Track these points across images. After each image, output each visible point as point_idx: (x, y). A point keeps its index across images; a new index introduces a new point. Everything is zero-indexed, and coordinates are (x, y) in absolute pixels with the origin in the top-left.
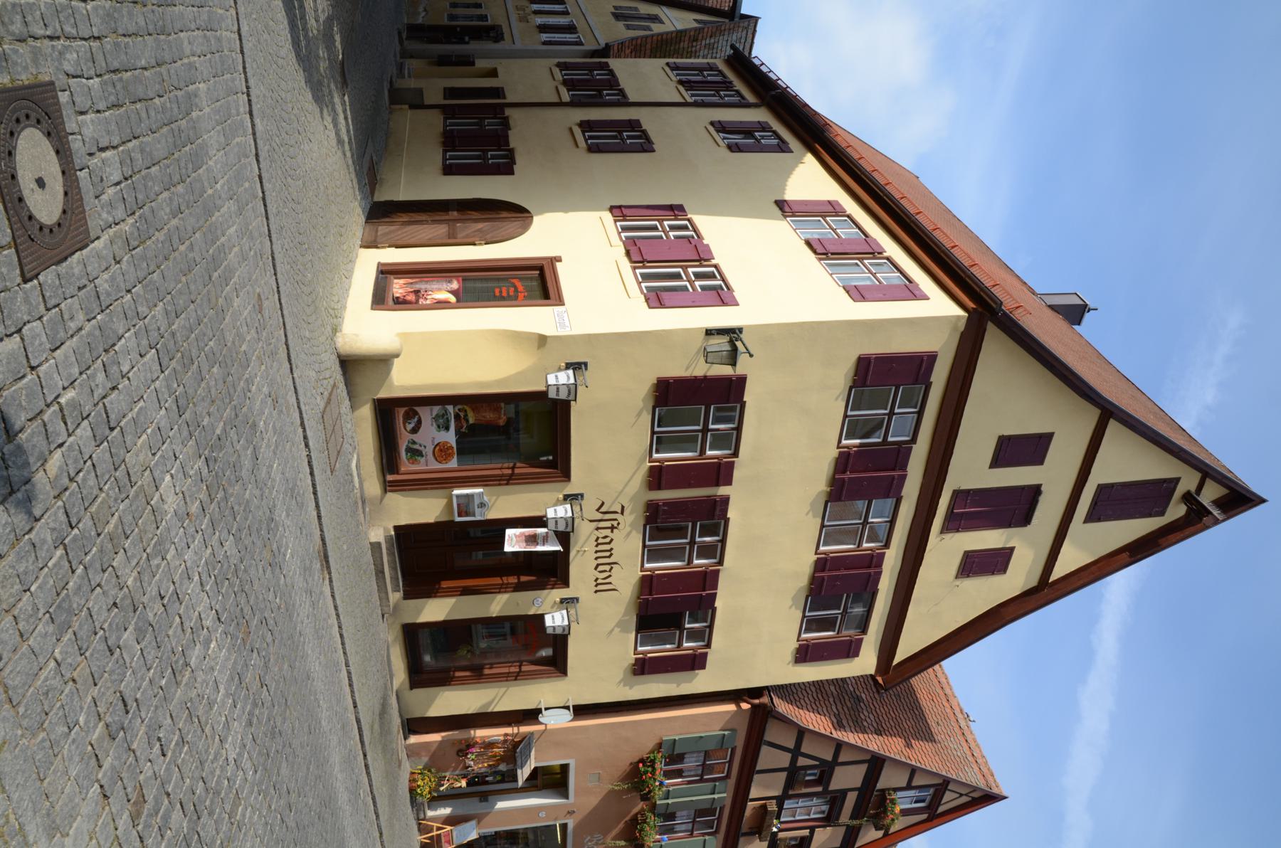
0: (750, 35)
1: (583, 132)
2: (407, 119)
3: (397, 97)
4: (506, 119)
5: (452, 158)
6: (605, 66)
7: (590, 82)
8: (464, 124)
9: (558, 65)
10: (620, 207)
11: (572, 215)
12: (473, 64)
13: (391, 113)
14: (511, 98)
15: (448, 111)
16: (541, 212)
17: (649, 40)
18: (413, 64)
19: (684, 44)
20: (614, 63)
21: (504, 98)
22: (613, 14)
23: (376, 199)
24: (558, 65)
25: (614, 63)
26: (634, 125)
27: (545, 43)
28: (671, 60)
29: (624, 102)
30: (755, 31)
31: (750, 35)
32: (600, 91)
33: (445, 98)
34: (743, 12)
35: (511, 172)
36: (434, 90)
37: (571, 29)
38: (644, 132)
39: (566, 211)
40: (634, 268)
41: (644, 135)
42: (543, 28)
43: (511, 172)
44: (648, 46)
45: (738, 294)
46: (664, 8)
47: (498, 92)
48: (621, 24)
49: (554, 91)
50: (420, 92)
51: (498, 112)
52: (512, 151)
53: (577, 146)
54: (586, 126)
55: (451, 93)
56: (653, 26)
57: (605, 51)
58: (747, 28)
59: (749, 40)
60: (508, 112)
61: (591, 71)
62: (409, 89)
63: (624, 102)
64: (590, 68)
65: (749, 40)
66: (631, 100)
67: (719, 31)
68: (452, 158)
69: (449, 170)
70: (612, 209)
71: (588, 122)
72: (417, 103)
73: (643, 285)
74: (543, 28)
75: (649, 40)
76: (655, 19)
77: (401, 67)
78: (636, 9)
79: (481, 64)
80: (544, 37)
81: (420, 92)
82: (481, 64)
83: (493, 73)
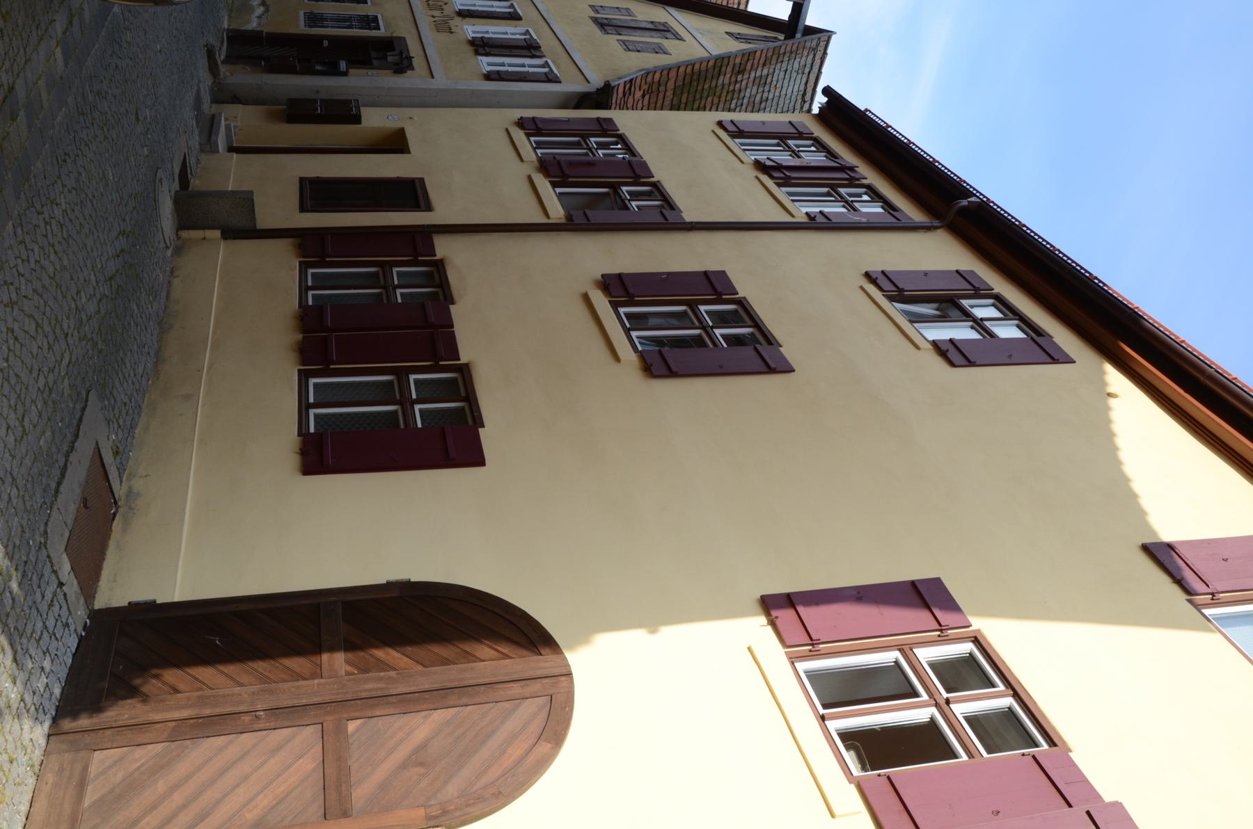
0: (818, 61)
1: (615, 306)
2: (217, 267)
3: (196, 210)
4: (440, 265)
5: (321, 282)
6: (605, 127)
7: (597, 184)
8: (350, 282)
9: (521, 123)
10: (790, 600)
11: (676, 636)
12: (357, 119)
13: (178, 251)
14: (442, 213)
15: (313, 246)
16: (583, 637)
17: (673, 74)
18: (241, 120)
19: (725, 79)
20: (627, 121)
21: (429, 208)
22: (595, 20)
23: (99, 604)
24: (521, 123)
25: (627, 121)
26: (714, 285)
27: (488, 77)
28: (726, 116)
29: (666, 218)
30: (825, 53)
31: (818, 61)
32: (615, 187)
33: (303, 209)
34: (786, 18)
35: (473, 456)
36: (275, 191)
37: (530, 48)
38: (656, 186)
39: (652, 623)
40: (793, 660)
41: (744, 312)
42: (482, 46)
43: (473, 456)
44: (671, 85)
45: (789, 351)
46: (673, 11)
47: (410, 193)
48: (612, 40)
49: (505, 134)
50: (245, 201)
51: (418, 242)
52: (465, 371)
53: (617, 359)
54: (619, 288)
55: (318, 193)
56: (668, 44)
57: (601, 97)
58: (815, 50)
59: (815, 70)
60: (444, 247)
61: (585, 137)
62: (221, 195)
63: (666, 218)
64: (583, 132)
65: (815, 70)
66: (688, 217)
67: (776, 56)
68: (321, 282)
69: (325, 452)
70: (769, 604)
71: (620, 277)
72: (241, 227)
73: (634, 334)
74: (482, 46)
75: (673, 74)
76: (663, 30)
77: (209, 127)
78: (628, 12)
79: (375, 119)
80: (486, 63)
81: (245, 201)
82: (375, 119)
83: (396, 143)
